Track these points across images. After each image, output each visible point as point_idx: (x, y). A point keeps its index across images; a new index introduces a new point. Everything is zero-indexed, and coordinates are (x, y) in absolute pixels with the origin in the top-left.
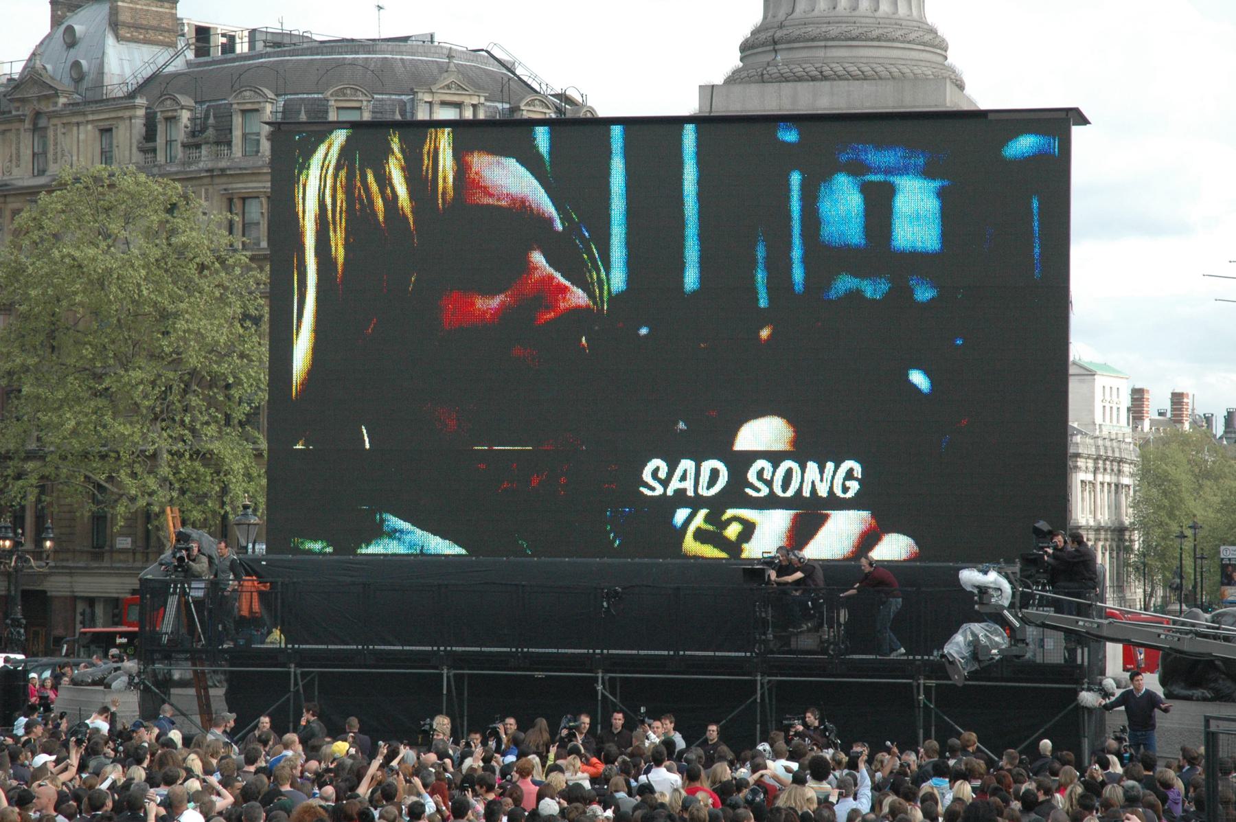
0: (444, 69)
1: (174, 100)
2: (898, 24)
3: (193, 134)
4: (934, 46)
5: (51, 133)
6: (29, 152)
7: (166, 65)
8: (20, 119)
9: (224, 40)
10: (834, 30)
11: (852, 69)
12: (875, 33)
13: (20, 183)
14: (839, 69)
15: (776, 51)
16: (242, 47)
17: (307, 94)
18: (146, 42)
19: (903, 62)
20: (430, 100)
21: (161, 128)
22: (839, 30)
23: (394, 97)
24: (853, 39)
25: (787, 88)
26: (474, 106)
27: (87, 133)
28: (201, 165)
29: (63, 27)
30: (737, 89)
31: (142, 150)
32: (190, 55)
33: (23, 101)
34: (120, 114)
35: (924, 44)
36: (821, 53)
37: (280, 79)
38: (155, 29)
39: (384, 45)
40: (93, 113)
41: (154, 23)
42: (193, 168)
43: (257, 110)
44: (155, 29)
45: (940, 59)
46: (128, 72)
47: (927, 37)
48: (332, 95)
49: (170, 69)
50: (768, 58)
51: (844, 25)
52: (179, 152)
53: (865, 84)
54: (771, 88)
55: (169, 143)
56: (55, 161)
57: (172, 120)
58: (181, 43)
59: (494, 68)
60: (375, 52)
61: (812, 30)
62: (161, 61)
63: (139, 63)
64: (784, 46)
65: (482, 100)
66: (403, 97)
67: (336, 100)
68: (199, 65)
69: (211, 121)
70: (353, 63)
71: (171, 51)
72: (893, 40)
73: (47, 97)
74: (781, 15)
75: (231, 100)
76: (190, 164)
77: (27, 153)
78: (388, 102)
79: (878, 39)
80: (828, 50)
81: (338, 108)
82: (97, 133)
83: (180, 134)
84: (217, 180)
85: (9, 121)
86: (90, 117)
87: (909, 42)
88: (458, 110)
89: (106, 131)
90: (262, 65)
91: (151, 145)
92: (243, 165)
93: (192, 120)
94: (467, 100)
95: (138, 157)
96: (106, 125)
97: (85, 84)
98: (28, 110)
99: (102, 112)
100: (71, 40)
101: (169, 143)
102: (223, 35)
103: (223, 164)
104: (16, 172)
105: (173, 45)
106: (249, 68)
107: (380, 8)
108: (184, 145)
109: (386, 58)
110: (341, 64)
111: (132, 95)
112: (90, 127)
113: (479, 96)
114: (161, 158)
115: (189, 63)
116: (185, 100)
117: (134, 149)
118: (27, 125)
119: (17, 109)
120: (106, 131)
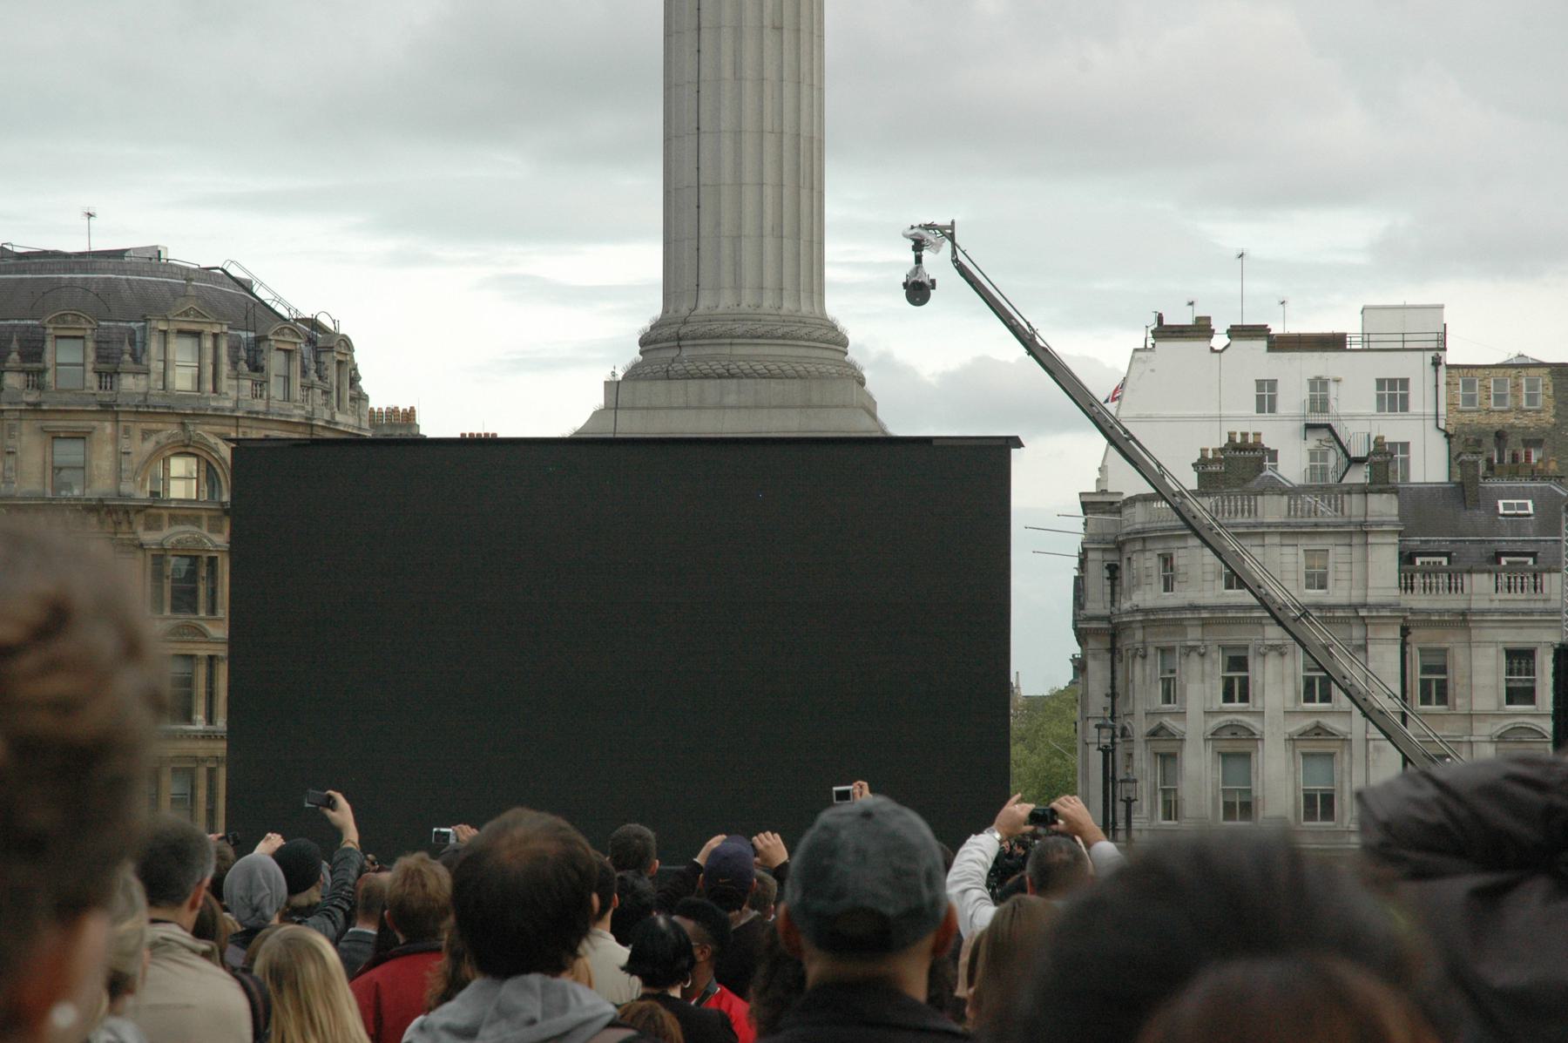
0: (176, 292)
2: (802, 322)
10: (739, 328)
12: (780, 332)
17: (19, 319)
19: (807, 360)
20: (165, 328)
22: (745, 328)
23: (121, 324)
24: (759, 337)
25: (693, 386)
26: (215, 336)
30: (643, 386)
35: (828, 342)
36: (727, 350)
39: (104, 262)
45: (839, 356)
48: (49, 322)
50: (673, 353)
51: (750, 323)
53: (773, 383)
54: (678, 386)
60: (94, 271)
64: (689, 342)
65: (225, 328)
66: (132, 324)
67: (55, 328)
70: (71, 283)
72: (798, 339)
74: (684, 310)
78: (115, 330)
79: (783, 337)
80: (734, 347)
81: (57, 337)
87: (814, 340)
88: (197, 339)
94: (208, 329)
109: (109, 278)
110: (57, 286)
113: (221, 324)
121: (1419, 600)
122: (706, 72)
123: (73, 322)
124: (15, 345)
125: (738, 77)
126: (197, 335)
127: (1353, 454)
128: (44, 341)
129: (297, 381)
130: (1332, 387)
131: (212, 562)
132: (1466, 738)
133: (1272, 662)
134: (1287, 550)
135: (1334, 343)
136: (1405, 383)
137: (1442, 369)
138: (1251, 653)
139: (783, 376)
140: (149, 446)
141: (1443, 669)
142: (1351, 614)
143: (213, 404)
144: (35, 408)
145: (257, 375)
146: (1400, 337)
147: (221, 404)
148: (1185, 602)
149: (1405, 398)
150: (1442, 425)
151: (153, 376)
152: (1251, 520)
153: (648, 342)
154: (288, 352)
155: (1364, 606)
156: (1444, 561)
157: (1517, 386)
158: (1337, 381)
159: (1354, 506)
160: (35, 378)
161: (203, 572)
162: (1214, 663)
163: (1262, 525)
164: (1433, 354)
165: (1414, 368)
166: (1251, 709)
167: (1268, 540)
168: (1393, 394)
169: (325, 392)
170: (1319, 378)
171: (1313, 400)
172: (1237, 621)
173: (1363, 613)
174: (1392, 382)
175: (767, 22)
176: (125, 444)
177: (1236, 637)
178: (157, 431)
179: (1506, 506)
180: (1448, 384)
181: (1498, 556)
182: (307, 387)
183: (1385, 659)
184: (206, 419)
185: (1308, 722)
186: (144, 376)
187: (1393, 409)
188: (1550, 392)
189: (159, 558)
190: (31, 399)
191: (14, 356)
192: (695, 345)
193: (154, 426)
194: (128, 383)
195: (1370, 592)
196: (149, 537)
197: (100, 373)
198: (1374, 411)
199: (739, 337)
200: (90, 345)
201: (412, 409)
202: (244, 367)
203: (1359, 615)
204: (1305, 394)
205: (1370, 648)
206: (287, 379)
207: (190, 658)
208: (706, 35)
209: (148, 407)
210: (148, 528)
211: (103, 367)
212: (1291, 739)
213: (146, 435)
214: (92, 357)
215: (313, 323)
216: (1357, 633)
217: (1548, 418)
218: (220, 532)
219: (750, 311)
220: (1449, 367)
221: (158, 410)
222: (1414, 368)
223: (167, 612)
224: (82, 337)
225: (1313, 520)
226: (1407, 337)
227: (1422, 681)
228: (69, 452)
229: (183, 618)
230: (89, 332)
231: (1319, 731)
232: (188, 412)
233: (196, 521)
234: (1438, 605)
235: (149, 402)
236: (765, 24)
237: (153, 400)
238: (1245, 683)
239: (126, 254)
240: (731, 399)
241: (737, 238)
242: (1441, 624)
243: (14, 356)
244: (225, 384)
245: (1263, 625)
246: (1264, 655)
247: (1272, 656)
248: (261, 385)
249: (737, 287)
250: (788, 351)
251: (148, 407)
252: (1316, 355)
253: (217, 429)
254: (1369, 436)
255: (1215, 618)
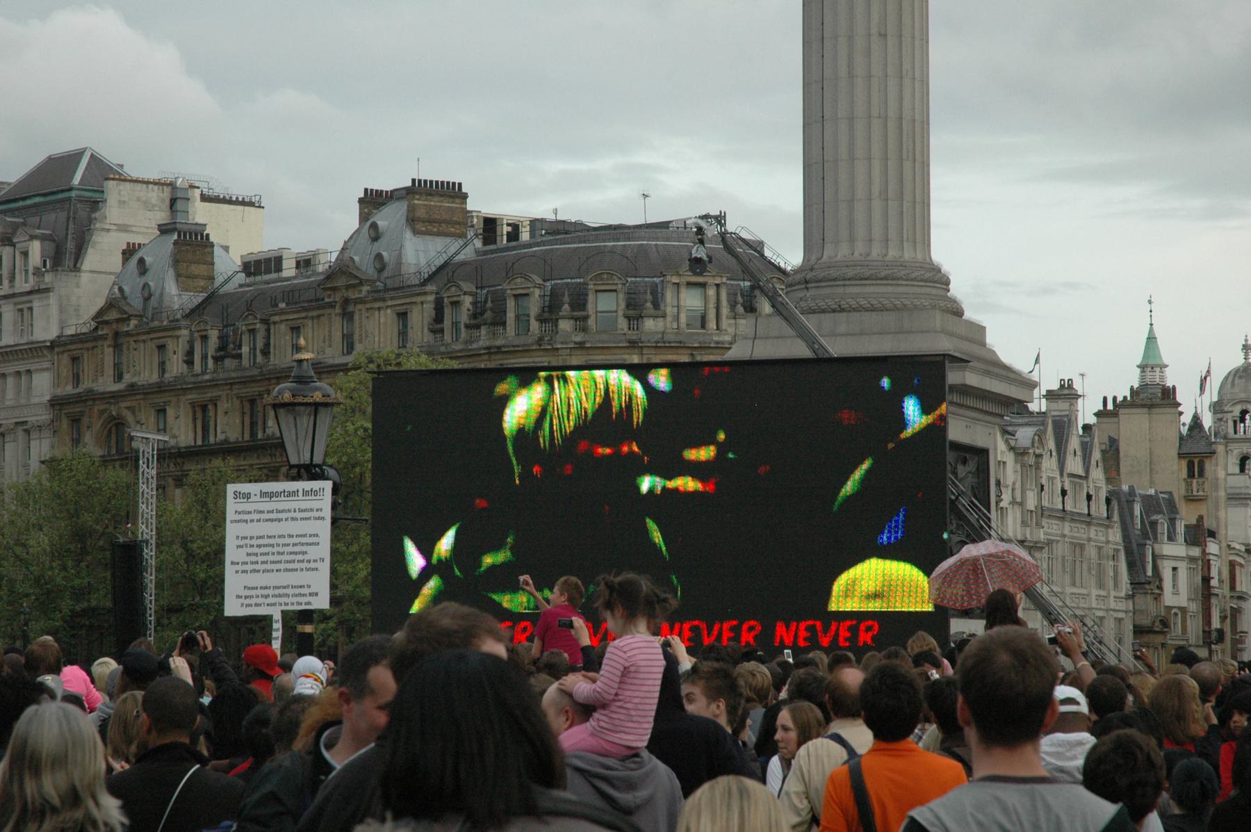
1: (458, 286)
3: (474, 316)
4: (935, 282)
5: (356, 317)
6: (339, 334)
7: (457, 253)
8: (331, 305)
9: (510, 229)
10: (851, 273)
11: (863, 302)
12: (883, 274)
13: (331, 361)
14: (853, 303)
15: (807, 288)
16: (525, 236)
17: (571, 278)
18: (439, 234)
19: (905, 296)
20: (678, 281)
21: (447, 311)
22: (854, 272)
23: (646, 279)
24: (866, 279)
26: (718, 286)
27: (386, 318)
28: (481, 343)
29: (370, 222)
31: (433, 331)
32: (478, 243)
33: (334, 289)
34: (414, 299)
35: (926, 281)
36: (841, 290)
37: (548, 267)
38: (448, 222)
39: (642, 232)
40: (392, 299)
41: (446, 217)
42: (475, 346)
43: (527, 295)
44: (448, 222)
45: (941, 292)
46: (423, 262)
47: (928, 275)
48: (591, 279)
49: (460, 257)
51: (859, 268)
52: (464, 333)
53: (874, 315)
55: (455, 324)
56: (361, 341)
57: (456, 304)
58: (470, 234)
60: (634, 239)
61: (833, 273)
62: (452, 250)
63: (433, 254)
64: (813, 285)
65: (724, 280)
66: (655, 279)
67: (594, 284)
68: (485, 253)
69: (489, 304)
70: (612, 251)
71: (461, 242)
72: (898, 279)
73: (353, 286)
75: (505, 286)
76: (471, 342)
77: (337, 336)
78: (642, 284)
79: (886, 278)
80: (847, 288)
81: (597, 291)
82: (395, 316)
83: (464, 318)
84: (493, 357)
85: (323, 307)
86: (390, 303)
87: (912, 280)
88: (703, 289)
89: (403, 316)
90: (533, 255)
91: (439, 326)
92: (516, 342)
93: (474, 304)
94: (710, 281)
95: (428, 337)
96: (402, 309)
97: (385, 274)
98: (338, 297)
99: (399, 298)
100: (376, 234)
101: (455, 324)
102: (508, 225)
103: (499, 342)
104: (328, 351)
105: (462, 236)
106: (524, 256)
108: (467, 326)
109: (642, 244)
110: (600, 251)
111: (425, 283)
112: (389, 311)
113: (721, 276)
114: (447, 337)
115: (477, 252)
116: (467, 286)
117: (426, 330)
118: (338, 310)
119: (329, 296)
120: (403, 316)
123: (608, 279)
124: (566, 299)
125: (851, 76)
126: (703, 285)
128: (587, 295)
139: (883, 309)
143: (716, 338)
147: (721, 338)
151: (669, 319)
160: (581, 322)
175: (874, 31)
184: (710, 351)
186: (662, 319)
190: (578, 339)
191: (566, 307)
192: (818, 287)
194: (649, 324)
197: (628, 318)
199: (849, 279)
200: (621, 296)
202: (740, 309)
208: (827, 43)
209: (664, 342)
211: (631, 313)
214: (623, 305)
219: (880, 258)
221: (672, 345)
224: (615, 291)
230: (620, 286)
232: (696, 345)
235: (665, 339)
236: (872, 32)
237: (667, 338)
239: (670, 225)
240: (842, 328)
241: (851, 201)
243: (566, 307)
244: (725, 323)
249: (852, 240)
250: (890, 289)
251: (664, 342)
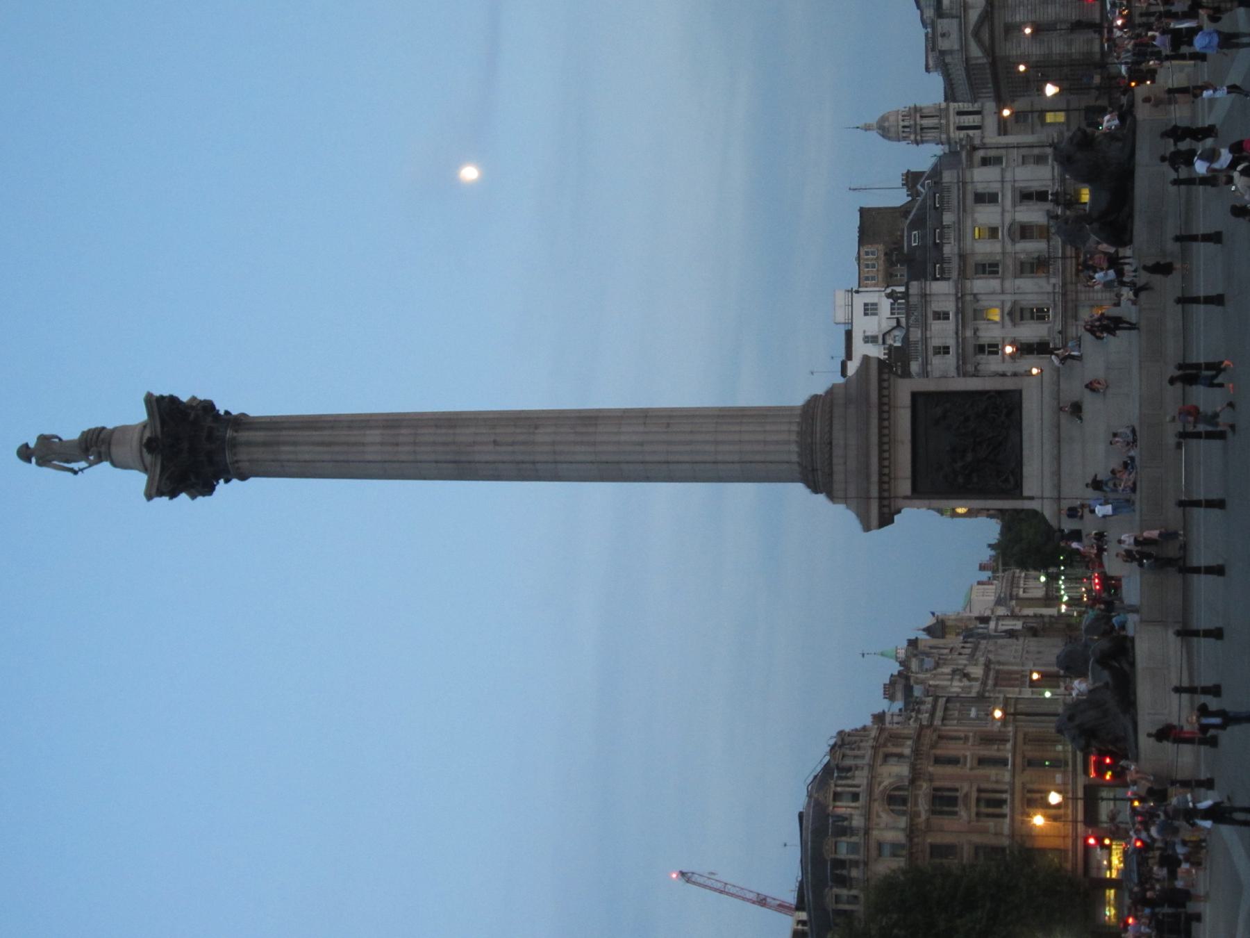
25: (835, 461)
50: (819, 472)
54: (836, 468)
59: (817, 781)
65: (832, 781)
107: (785, 845)
121: (955, 274)
122: (686, 458)
124: (838, 872)
125: (690, 443)
127: (895, 324)
129: (856, 752)
130: (869, 334)
131: (935, 789)
132: (1013, 255)
133: (980, 334)
134: (933, 328)
135: (849, 335)
136: (866, 305)
137: (861, 289)
138: (978, 343)
140: (884, 815)
141: (984, 265)
142: (960, 301)
144: (866, 864)
145: (853, 769)
146: (847, 307)
148: (955, 371)
149: (872, 304)
150: (883, 289)
151: (853, 812)
152: (920, 343)
153: (815, 489)
154: (844, 756)
155: (956, 294)
156: (938, 266)
157: (867, 260)
158: (864, 332)
159: (914, 300)
161: (939, 793)
162: (982, 359)
163: (922, 338)
164: (854, 294)
165: (859, 301)
166: (1001, 342)
167: (928, 336)
168: (870, 309)
169: (862, 741)
170: (864, 339)
171: (872, 342)
172: (962, 349)
173: (960, 295)
174: (865, 310)
176: (882, 825)
177: (970, 350)
178: (877, 813)
179: (915, 242)
180: (866, 287)
181: (935, 243)
182: (859, 748)
183: (980, 285)
185: (1007, 318)
187: (876, 309)
188: (870, 246)
189: (934, 812)
191: (845, 872)
193: (875, 813)
195: (951, 292)
196: (923, 816)
197: (852, 835)
198: (876, 317)
200: (839, 839)
201: (872, 715)
202: (849, 774)
203: (960, 298)
204: (870, 345)
205: (975, 291)
206: (856, 757)
207: (978, 800)
210: (919, 816)
212: (1015, 325)
213: (878, 816)
215: (833, 747)
216: (968, 298)
217: (881, 247)
218: (921, 786)
220: (859, 286)
222: (859, 301)
223: (957, 809)
225: (920, 317)
226: (847, 304)
227: (989, 274)
228: (887, 851)
229: (960, 802)
231: (1011, 314)
233: (916, 797)
234: (957, 266)
238: (990, 346)
241: (765, 443)
242: (965, 265)
244: (856, 782)
245: (965, 338)
246: (978, 337)
247: (978, 334)
248: (857, 767)
252: (854, 340)
253: (876, 786)
254: (888, 318)
255: (962, 358)
